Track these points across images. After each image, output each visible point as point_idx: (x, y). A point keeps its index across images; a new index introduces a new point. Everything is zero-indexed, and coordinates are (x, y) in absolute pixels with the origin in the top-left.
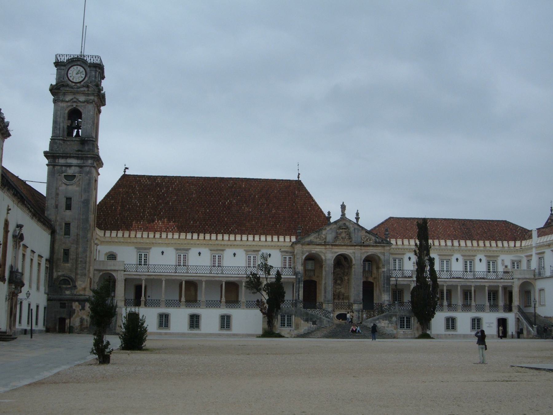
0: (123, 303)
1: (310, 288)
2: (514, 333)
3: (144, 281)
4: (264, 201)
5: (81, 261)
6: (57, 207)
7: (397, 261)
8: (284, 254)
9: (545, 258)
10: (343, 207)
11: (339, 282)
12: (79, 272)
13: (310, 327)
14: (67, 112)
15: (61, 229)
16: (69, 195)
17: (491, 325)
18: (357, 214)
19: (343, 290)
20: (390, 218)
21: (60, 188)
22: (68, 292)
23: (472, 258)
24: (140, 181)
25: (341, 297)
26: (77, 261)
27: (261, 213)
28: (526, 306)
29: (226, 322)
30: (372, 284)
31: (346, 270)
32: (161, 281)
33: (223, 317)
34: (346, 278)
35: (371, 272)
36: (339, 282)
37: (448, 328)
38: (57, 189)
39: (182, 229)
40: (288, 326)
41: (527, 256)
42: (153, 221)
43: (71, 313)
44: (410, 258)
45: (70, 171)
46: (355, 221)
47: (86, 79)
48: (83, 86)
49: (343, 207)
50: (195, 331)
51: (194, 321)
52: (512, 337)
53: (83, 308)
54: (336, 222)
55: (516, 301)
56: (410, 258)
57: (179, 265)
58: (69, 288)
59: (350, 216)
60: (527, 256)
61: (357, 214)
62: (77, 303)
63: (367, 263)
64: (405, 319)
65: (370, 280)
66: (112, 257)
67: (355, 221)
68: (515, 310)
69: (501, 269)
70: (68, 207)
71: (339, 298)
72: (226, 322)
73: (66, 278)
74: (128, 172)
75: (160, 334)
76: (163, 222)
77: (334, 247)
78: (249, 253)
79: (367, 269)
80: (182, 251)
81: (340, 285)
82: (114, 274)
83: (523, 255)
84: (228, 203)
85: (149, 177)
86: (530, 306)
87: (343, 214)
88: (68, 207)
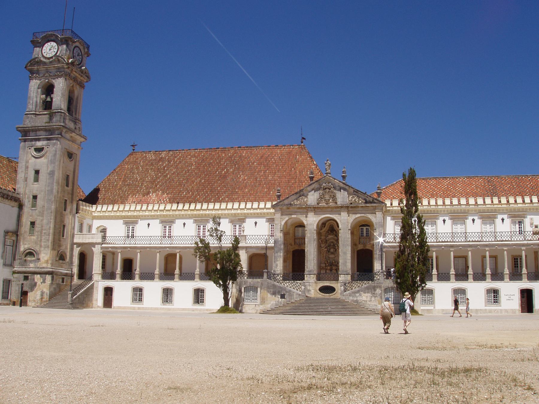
5: (45, 233)
6: (26, 180)
11: (332, 250)
12: (43, 244)
13: (278, 301)
15: (29, 201)
16: (37, 168)
17: (512, 297)
21: (30, 161)
22: (32, 265)
24: (146, 156)
25: (334, 268)
26: (41, 233)
27: (256, 179)
36: (332, 250)
38: (27, 162)
42: (148, 193)
43: (34, 286)
45: (39, 144)
47: (59, 52)
50: (168, 306)
53: (44, 281)
57: (165, 237)
58: (34, 260)
62: (39, 276)
63: (365, 228)
70: (36, 180)
73: (31, 251)
75: (134, 308)
76: (157, 195)
80: (167, 222)
81: (332, 253)
84: (225, 173)
88: (36, 180)
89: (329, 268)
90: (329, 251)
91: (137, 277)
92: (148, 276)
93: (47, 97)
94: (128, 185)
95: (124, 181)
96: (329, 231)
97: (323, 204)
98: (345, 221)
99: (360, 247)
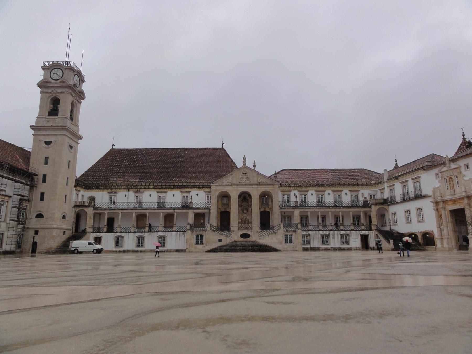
0: (91, 230)
1: (224, 218)
2: (374, 246)
3: (106, 215)
4: (199, 161)
7: (286, 196)
8: (207, 193)
9: (395, 189)
10: (244, 159)
11: (245, 211)
14: (50, 99)
17: (357, 240)
18: (255, 163)
19: (248, 217)
20: (284, 169)
23: (339, 193)
25: (247, 222)
28: (382, 226)
29: (163, 241)
30: (269, 212)
31: (250, 204)
32: (118, 213)
33: (160, 237)
34: (250, 209)
35: (267, 204)
36: (245, 211)
37: (323, 243)
40: (201, 243)
41: (380, 190)
42: (124, 176)
44: (295, 194)
46: (253, 168)
48: (61, 82)
49: (244, 159)
52: (373, 249)
54: (240, 169)
55: (374, 221)
56: (295, 194)
59: (250, 164)
60: (380, 190)
61: (255, 163)
64: (288, 237)
65: (267, 210)
66: (92, 199)
67: (253, 168)
68: (373, 228)
69: (361, 200)
71: (245, 223)
74: (114, 147)
77: (238, 187)
78: (184, 194)
79: (265, 202)
82: (86, 209)
83: (377, 190)
85: (127, 150)
86: (386, 226)
87: (245, 164)
89: (245, 223)
90: (243, 212)
93: (54, 106)
95: (106, 168)
97: (243, 183)
98: (255, 193)
99: (262, 210)
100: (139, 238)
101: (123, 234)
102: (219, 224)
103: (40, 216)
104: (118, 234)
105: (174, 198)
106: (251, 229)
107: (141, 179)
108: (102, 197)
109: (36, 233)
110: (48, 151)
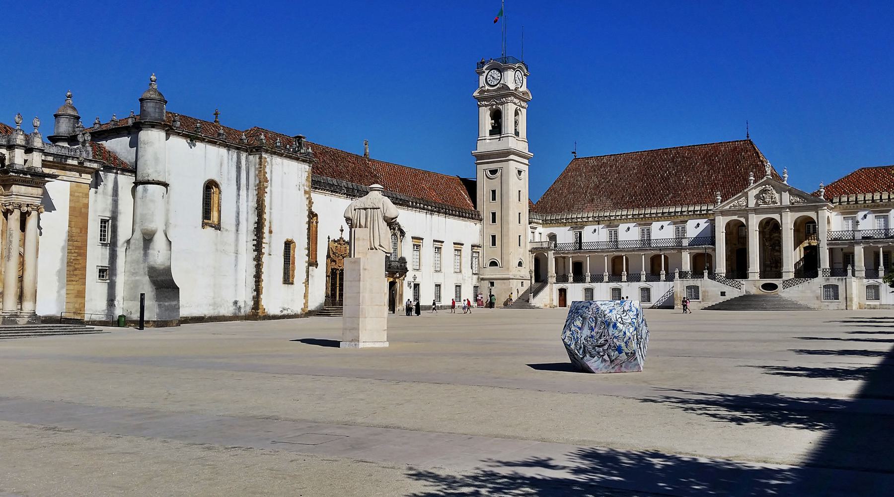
0: (554, 280)
29: (646, 294)
33: (643, 289)
39: (616, 206)
42: (593, 200)
51: (617, 294)
66: (553, 237)
72: (646, 294)
89: (772, 265)
91: (588, 279)
92: (597, 278)
94: (573, 193)
96: (771, 232)
100: (614, 290)
101: (594, 285)
102: (735, 267)
103: (493, 264)
104: (587, 285)
105: (663, 232)
106: (779, 275)
107: (618, 205)
108: (565, 236)
109: (492, 284)
110: (495, 184)
